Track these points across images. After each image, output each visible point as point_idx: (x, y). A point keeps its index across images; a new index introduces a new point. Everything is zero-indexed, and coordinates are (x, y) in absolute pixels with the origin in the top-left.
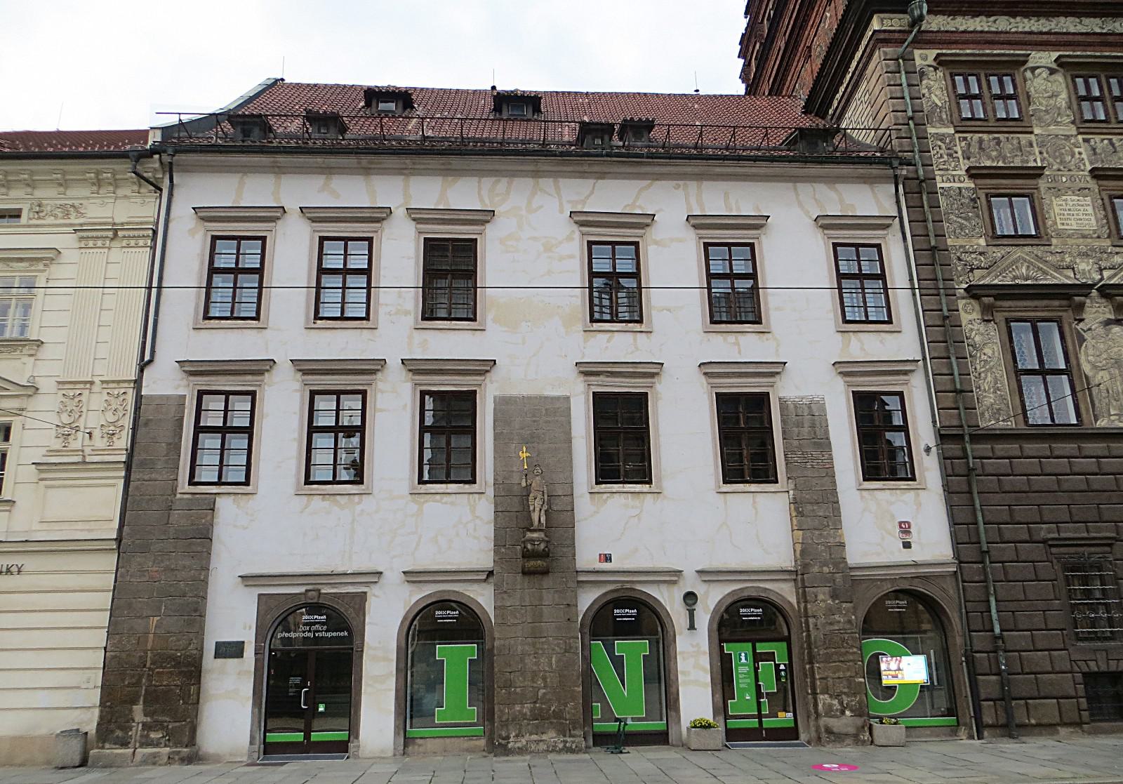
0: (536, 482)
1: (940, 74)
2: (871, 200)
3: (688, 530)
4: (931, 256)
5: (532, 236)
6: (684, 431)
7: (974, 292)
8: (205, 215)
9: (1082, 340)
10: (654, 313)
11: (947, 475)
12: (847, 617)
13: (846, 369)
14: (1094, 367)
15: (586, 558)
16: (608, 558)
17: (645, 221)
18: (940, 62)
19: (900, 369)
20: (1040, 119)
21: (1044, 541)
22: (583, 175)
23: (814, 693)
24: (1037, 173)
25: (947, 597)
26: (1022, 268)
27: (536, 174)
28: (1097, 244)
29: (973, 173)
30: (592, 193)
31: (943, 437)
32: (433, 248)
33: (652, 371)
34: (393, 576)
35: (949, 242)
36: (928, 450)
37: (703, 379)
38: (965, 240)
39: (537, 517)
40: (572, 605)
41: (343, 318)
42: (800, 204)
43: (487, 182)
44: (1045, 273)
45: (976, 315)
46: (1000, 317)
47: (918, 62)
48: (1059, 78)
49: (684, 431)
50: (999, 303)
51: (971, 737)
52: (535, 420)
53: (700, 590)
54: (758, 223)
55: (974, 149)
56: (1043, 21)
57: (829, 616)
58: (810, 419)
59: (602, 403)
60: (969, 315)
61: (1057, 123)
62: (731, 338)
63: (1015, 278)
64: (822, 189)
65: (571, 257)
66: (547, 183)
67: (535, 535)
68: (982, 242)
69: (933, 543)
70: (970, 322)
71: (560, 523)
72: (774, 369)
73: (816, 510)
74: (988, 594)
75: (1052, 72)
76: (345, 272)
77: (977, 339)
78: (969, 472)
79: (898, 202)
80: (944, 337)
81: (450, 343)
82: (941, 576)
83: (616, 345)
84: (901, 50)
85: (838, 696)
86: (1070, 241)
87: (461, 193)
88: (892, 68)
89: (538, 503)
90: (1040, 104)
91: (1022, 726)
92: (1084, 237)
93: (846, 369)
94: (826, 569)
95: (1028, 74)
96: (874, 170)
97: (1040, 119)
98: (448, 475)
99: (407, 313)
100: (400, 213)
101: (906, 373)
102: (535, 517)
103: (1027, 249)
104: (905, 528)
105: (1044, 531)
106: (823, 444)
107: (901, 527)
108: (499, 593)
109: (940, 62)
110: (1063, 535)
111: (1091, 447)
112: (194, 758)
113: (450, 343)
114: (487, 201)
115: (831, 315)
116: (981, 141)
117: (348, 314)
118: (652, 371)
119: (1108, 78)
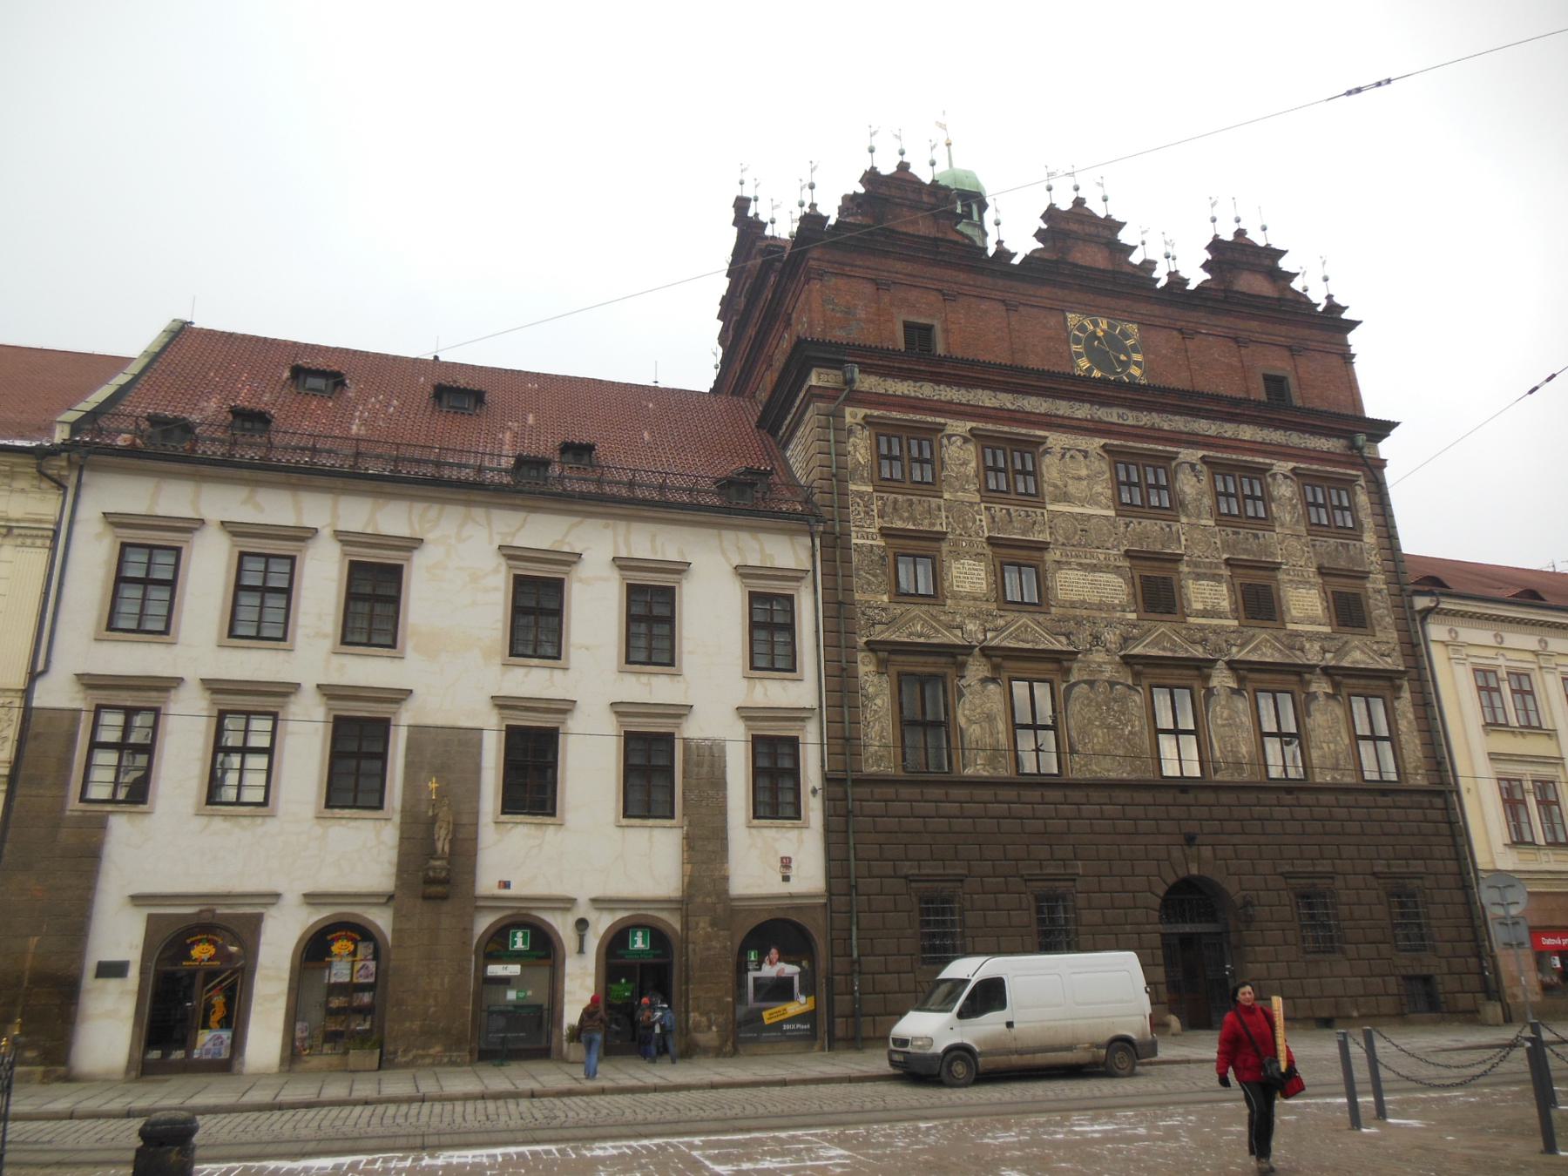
0: (443, 813)
1: (866, 433)
2: (786, 552)
3: (588, 860)
4: (838, 611)
5: (459, 569)
6: (590, 766)
7: (872, 646)
8: (114, 520)
9: (961, 695)
10: (572, 650)
11: (828, 816)
12: (724, 944)
13: (747, 714)
14: (969, 720)
15: (486, 883)
16: (506, 885)
17: (572, 559)
18: (868, 422)
19: (797, 715)
20: (950, 485)
21: (906, 877)
22: (514, 507)
23: (687, 1012)
24: (940, 537)
25: (817, 928)
26: (917, 627)
27: (469, 503)
28: (985, 607)
29: (885, 533)
30: (523, 526)
31: (828, 780)
32: (356, 570)
33: (565, 708)
34: (292, 897)
35: (857, 596)
36: (814, 792)
37: (613, 717)
38: (871, 596)
39: (442, 845)
40: (468, 930)
41: (258, 637)
42: (723, 552)
43: (419, 507)
44: (937, 631)
45: (871, 668)
46: (893, 670)
47: (848, 419)
48: (971, 447)
49: (590, 766)
50: (893, 657)
51: (822, 1049)
52: (447, 749)
53: (592, 916)
54: (681, 568)
55: (889, 510)
56: (963, 391)
57: (707, 944)
58: (710, 760)
59: (514, 737)
60: (865, 667)
61: (965, 490)
62: (644, 679)
63: (911, 634)
64: (745, 538)
65: (496, 589)
66: (479, 513)
67: (438, 863)
68: (885, 598)
69: (810, 877)
70: (866, 674)
71: (464, 851)
72: (681, 712)
73: (706, 847)
74: (851, 924)
75: (966, 440)
76: (264, 590)
77: (871, 690)
78: (848, 814)
79: (813, 556)
80: (840, 688)
81: (368, 670)
82: (813, 907)
83: (532, 681)
84: (832, 406)
85: (706, 1013)
86: (963, 603)
87: (391, 518)
88: (824, 424)
89: (443, 833)
90: (952, 470)
91: (865, 1039)
92: (975, 599)
93: (747, 714)
94: (708, 900)
95: (945, 441)
96: (794, 525)
97: (950, 485)
98: (355, 800)
99: (325, 636)
100: (326, 532)
101: (803, 719)
102: (439, 845)
103: (924, 608)
104: (786, 863)
105: (908, 868)
106: (718, 782)
107: (778, 861)
108: (398, 916)
109: (868, 422)
110: (924, 872)
111: (956, 793)
112: (69, 1078)
113: (368, 670)
114: (417, 527)
115: (740, 662)
116: (895, 502)
117: (265, 633)
118: (565, 708)
119: (1012, 451)
